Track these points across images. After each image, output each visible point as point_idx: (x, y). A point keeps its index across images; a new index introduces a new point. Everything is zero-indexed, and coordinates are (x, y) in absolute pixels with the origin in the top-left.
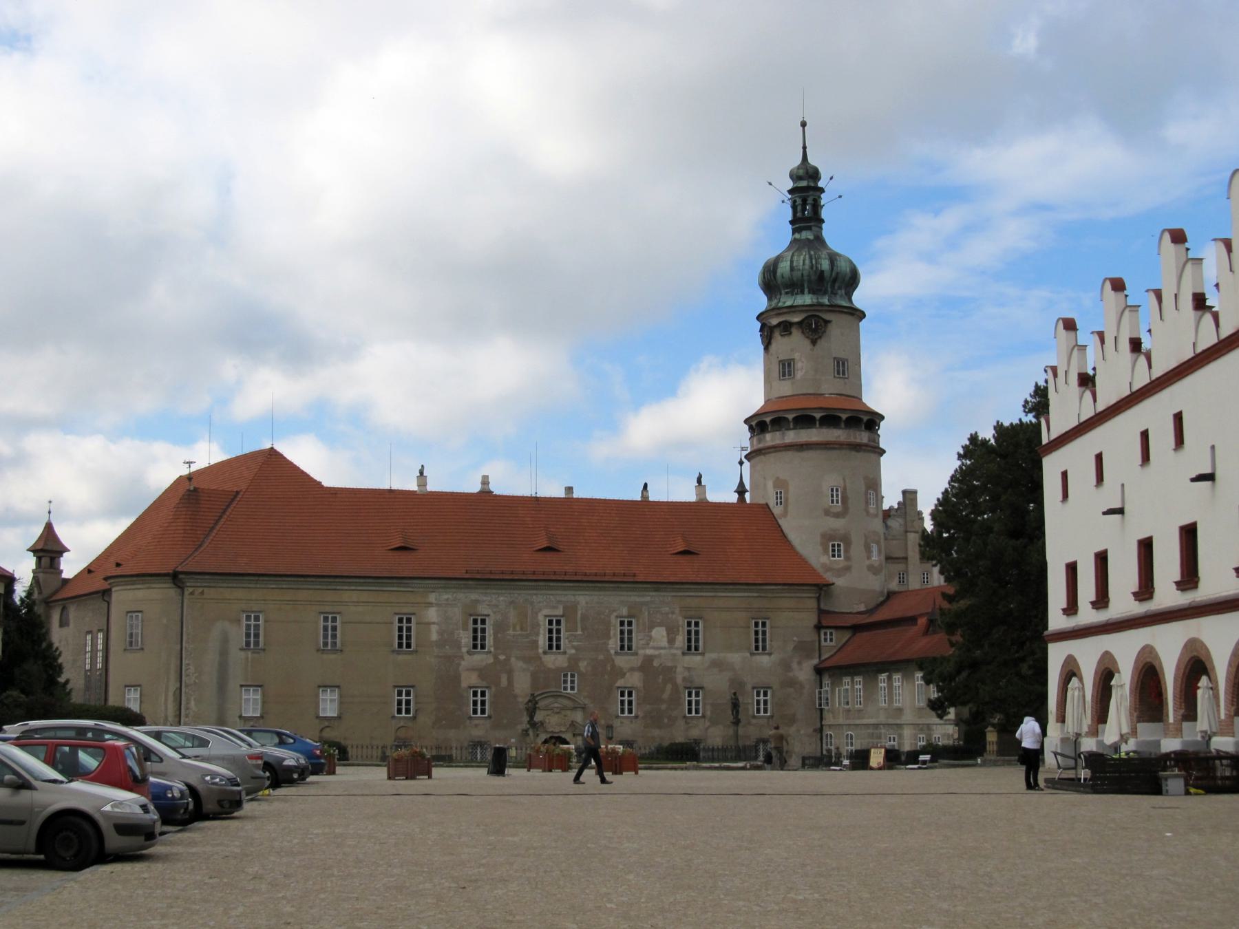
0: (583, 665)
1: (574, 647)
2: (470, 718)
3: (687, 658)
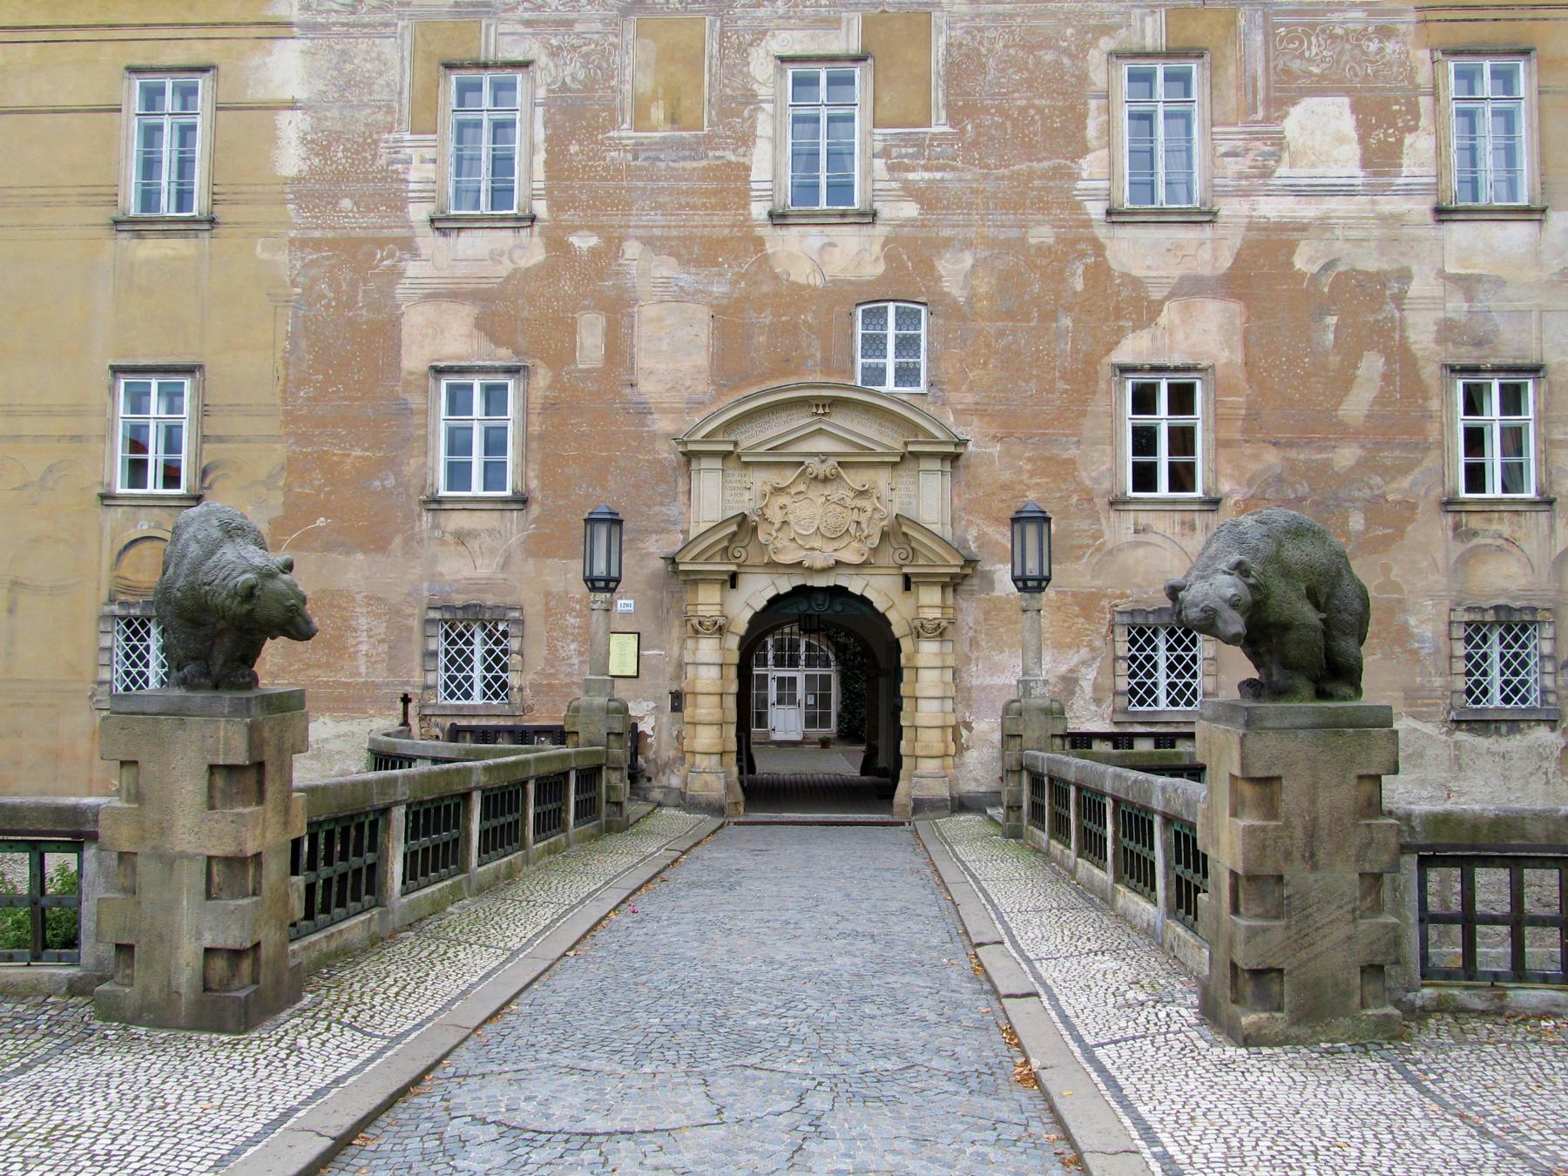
0: (954, 273)
2: (435, 504)
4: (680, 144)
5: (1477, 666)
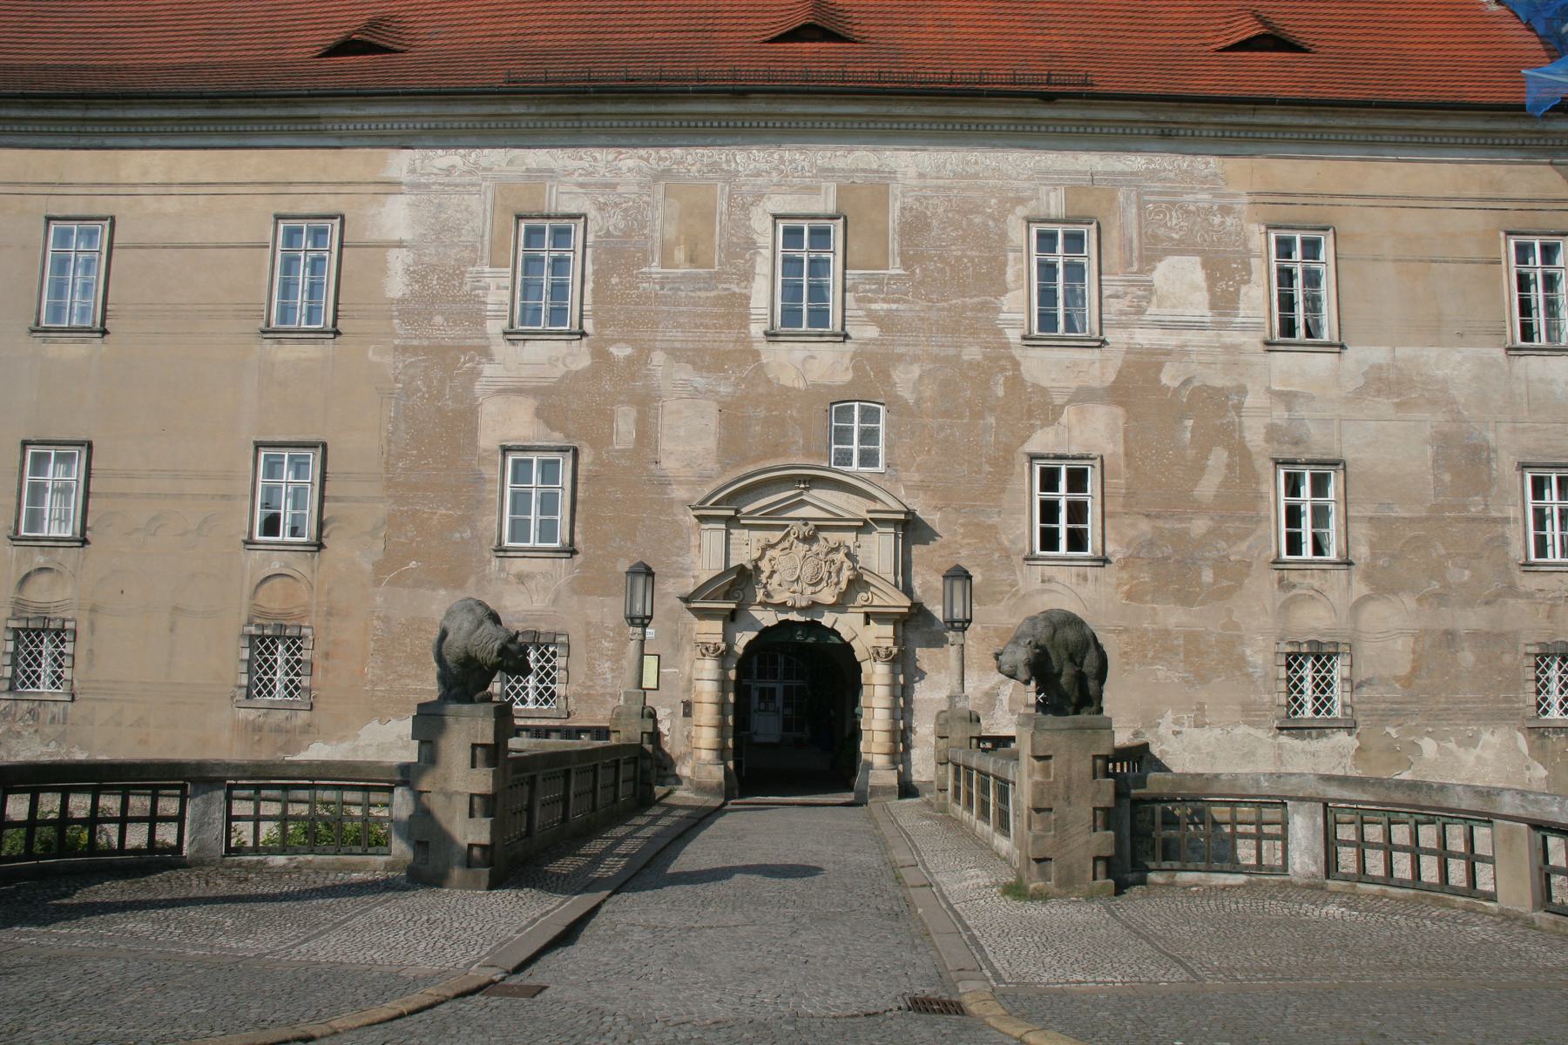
0: (906, 380)
1: (873, 318)
3: (1281, 359)
4: (694, 278)
5: (1295, 686)
